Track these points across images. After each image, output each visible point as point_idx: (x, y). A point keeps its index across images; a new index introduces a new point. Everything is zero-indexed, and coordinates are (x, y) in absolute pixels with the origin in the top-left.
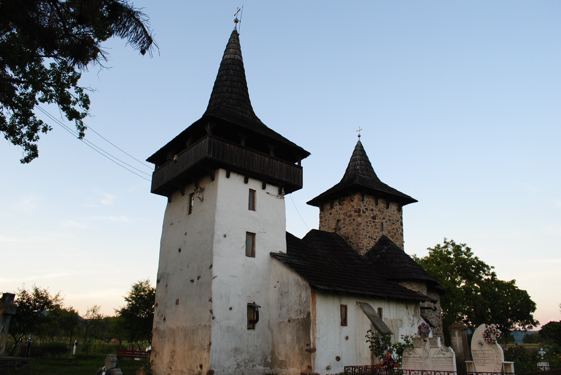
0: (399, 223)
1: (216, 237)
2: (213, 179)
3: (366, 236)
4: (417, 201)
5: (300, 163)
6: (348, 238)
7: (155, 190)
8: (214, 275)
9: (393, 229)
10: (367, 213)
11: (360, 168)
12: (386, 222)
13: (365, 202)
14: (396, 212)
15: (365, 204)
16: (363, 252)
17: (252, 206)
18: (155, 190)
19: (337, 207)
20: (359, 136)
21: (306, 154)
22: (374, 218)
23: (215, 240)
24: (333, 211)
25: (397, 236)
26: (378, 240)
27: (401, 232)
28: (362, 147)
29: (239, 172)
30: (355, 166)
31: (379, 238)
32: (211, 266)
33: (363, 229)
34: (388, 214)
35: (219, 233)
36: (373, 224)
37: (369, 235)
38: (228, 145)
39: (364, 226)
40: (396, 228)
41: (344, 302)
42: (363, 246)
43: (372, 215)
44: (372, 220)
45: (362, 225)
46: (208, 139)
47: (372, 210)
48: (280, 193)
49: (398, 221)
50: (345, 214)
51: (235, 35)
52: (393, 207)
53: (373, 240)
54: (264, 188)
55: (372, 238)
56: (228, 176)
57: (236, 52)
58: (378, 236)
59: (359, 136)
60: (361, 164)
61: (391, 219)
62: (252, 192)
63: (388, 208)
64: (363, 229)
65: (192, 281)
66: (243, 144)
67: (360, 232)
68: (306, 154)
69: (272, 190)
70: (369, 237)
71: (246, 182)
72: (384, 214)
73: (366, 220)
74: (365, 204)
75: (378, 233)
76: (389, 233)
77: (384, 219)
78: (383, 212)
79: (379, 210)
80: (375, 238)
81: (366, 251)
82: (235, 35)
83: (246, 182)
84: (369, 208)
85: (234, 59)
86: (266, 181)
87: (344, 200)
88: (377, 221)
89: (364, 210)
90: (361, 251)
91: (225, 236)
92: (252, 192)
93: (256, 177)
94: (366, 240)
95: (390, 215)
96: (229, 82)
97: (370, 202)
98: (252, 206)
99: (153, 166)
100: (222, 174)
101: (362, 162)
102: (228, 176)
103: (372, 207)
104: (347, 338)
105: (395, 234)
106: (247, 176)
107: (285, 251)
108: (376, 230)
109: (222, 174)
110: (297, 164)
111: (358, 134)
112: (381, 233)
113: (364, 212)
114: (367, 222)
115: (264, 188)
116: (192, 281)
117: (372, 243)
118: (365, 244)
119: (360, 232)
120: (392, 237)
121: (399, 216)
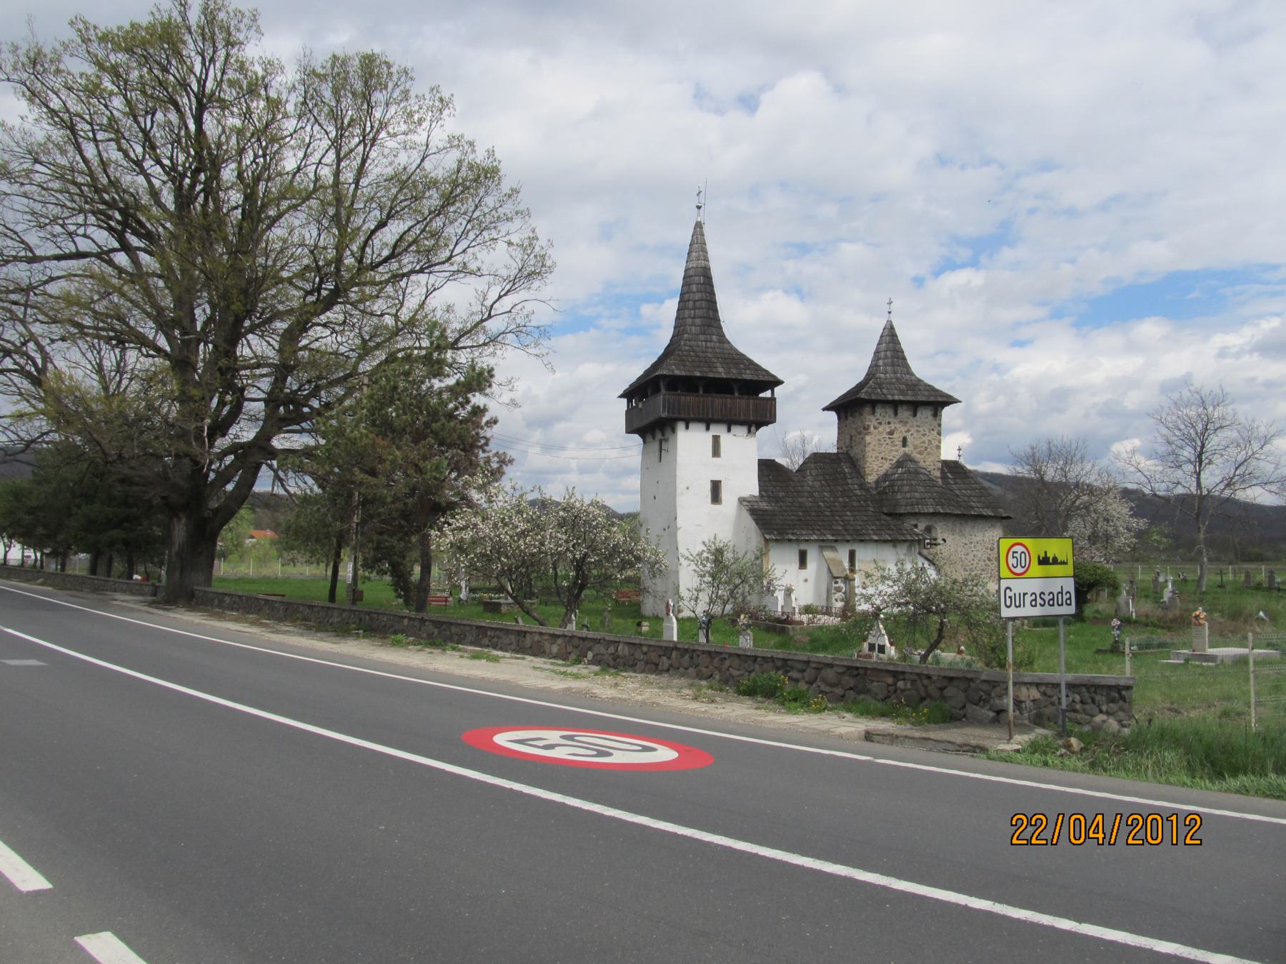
0: (935, 432)
1: (678, 491)
2: (674, 430)
3: (877, 457)
4: (960, 402)
5: (773, 393)
6: (857, 460)
7: (630, 430)
8: (679, 525)
9: (924, 442)
10: (881, 429)
11: (884, 363)
12: (912, 434)
13: (877, 415)
14: (931, 418)
15: (878, 417)
16: (871, 479)
17: (716, 452)
18: (630, 430)
19: (850, 419)
20: (890, 313)
21: (779, 382)
22: (891, 433)
23: (677, 493)
24: (848, 422)
25: (929, 450)
26: (895, 460)
27: (937, 443)
28: (892, 328)
29: (699, 420)
30: (878, 360)
31: (898, 457)
32: (676, 518)
33: (873, 450)
34: (915, 423)
35: (680, 486)
36: (888, 441)
37: (882, 455)
38: (683, 397)
39: (875, 446)
40: (929, 441)
41: (803, 547)
42: (873, 470)
43: (888, 430)
44: (887, 436)
45: (872, 445)
46: (662, 397)
47: (889, 423)
48: (749, 431)
49: (933, 430)
50: (856, 429)
51: (699, 226)
52: (925, 414)
53: (888, 462)
54: (729, 430)
55: (886, 459)
56: (687, 427)
57: (699, 256)
58: (897, 453)
59: (890, 313)
60: (886, 357)
61: (920, 429)
62: (716, 439)
63: (915, 415)
64: (873, 450)
65: (664, 530)
66: (701, 392)
67: (869, 454)
68: (779, 382)
69: (740, 431)
70: (882, 458)
71: (708, 429)
72: (908, 425)
73: (878, 437)
74: (878, 417)
75: (897, 451)
76: (915, 447)
77: (908, 431)
78: (907, 423)
79: (901, 422)
80: (891, 458)
81: (877, 477)
82: (699, 226)
83: (708, 429)
84: (883, 422)
85: (697, 267)
86: (730, 423)
87: (856, 411)
88: (895, 435)
89: (876, 424)
90: (869, 477)
91: (688, 488)
92: (716, 439)
93: (718, 421)
94: (877, 463)
95: (918, 424)
96: (691, 303)
97: (886, 413)
98: (716, 452)
99: (625, 401)
100: (681, 427)
101: (888, 353)
102: (687, 427)
103: (887, 420)
104: (806, 581)
105: (926, 448)
106: (708, 423)
107: (757, 493)
108: (894, 448)
109: (681, 427)
110: (767, 394)
111: (888, 310)
112: (902, 450)
113: (875, 428)
114: (879, 440)
115: (729, 430)
116: (664, 530)
117: (886, 466)
118: (876, 468)
119: (869, 454)
120: (920, 453)
121: (935, 423)
